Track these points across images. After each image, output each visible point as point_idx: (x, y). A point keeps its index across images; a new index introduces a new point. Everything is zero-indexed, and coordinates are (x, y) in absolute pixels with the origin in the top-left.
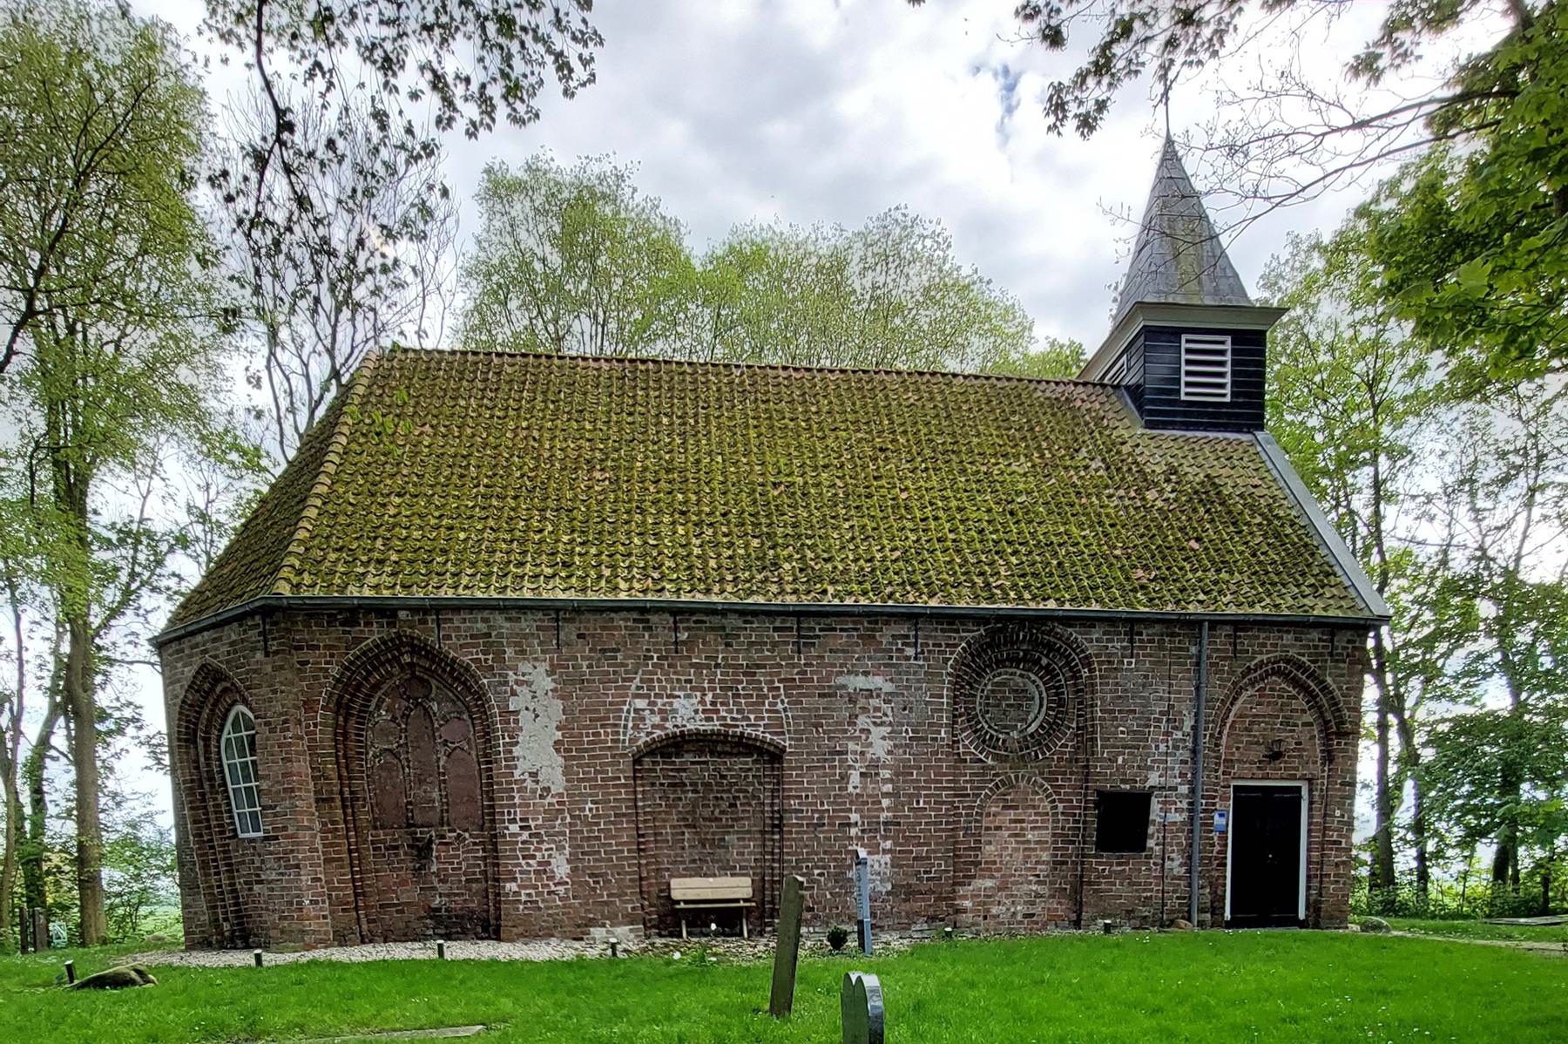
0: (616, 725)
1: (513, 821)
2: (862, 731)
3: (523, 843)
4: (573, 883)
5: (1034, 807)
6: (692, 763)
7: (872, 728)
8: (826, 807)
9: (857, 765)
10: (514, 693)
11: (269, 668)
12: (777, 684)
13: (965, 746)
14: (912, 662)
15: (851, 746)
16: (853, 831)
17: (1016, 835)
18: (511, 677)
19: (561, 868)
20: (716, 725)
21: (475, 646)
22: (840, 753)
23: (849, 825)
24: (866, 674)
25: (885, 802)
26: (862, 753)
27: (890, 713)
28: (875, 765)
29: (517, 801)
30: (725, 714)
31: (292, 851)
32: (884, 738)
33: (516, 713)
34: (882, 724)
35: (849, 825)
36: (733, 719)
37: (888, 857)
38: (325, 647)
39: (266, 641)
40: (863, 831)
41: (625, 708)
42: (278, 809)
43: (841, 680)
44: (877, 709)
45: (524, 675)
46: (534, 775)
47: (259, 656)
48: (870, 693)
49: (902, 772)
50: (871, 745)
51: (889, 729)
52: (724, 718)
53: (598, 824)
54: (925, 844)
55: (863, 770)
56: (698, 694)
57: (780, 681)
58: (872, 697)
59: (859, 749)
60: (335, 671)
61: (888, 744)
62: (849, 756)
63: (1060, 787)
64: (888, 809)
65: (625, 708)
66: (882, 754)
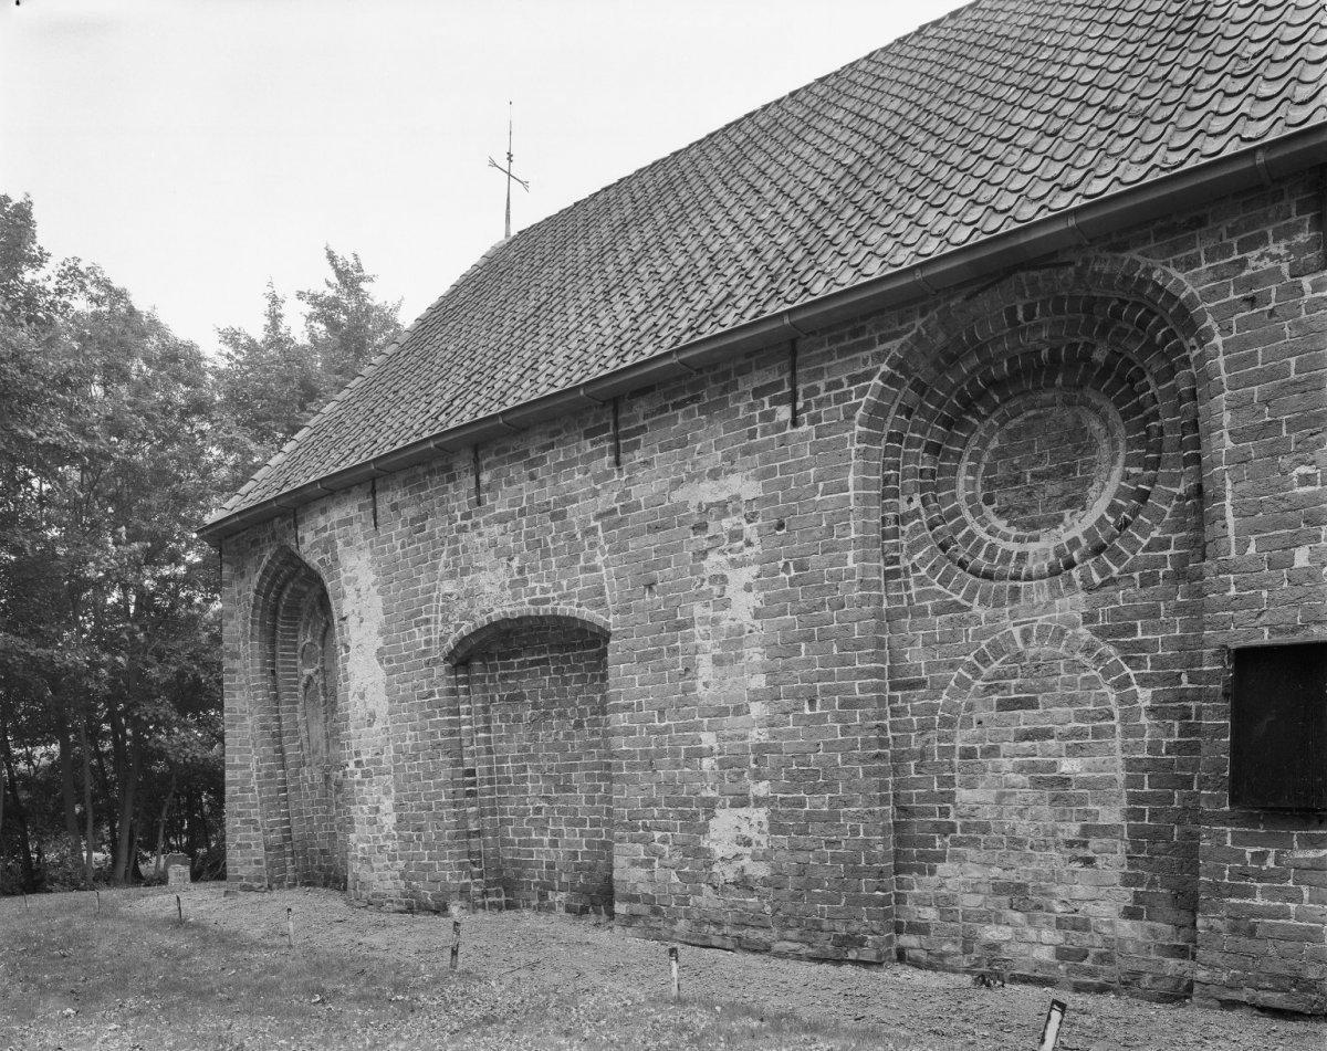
0: (427, 621)
2: (714, 579)
4: (400, 837)
5: (1072, 701)
7: (729, 574)
8: (667, 722)
9: (708, 644)
12: (593, 524)
13: (921, 581)
14: (788, 431)
15: (698, 610)
16: (707, 763)
17: (1034, 767)
19: (389, 821)
22: (681, 626)
23: (700, 754)
24: (715, 474)
25: (757, 709)
26: (715, 621)
27: (755, 539)
28: (736, 638)
30: (533, 585)
32: (748, 588)
34: (743, 564)
35: (700, 754)
36: (544, 590)
37: (761, 814)
40: (720, 762)
41: (435, 595)
43: (678, 496)
44: (736, 535)
48: (723, 508)
49: (784, 649)
50: (726, 605)
51: (755, 569)
52: (533, 591)
53: (416, 758)
54: (830, 786)
55: (718, 651)
56: (504, 560)
57: (599, 517)
58: (726, 514)
59: (710, 613)
61: (754, 600)
62: (698, 629)
63: (1141, 646)
64: (761, 723)
65: (435, 595)
66: (746, 618)
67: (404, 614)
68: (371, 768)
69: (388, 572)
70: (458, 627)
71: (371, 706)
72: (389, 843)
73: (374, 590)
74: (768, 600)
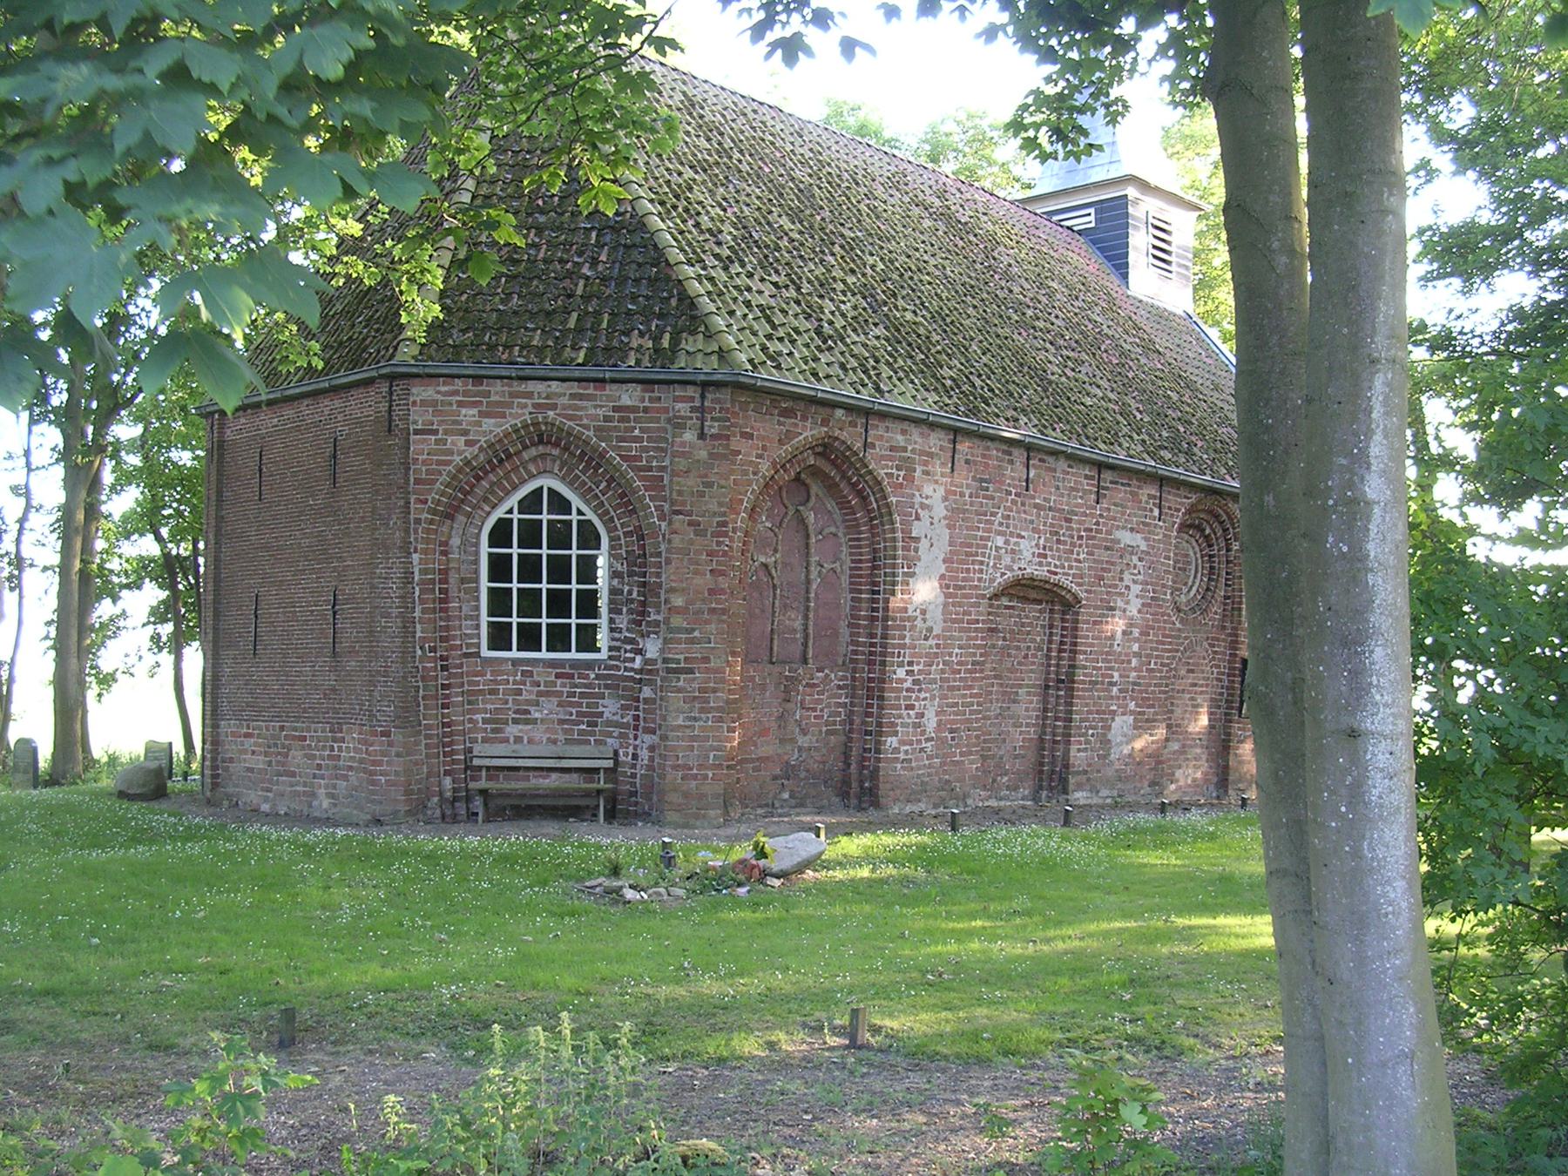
1: (901, 665)
3: (908, 690)
6: (1007, 607)
10: (918, 518)
11: (703, 454)
18: (917, 499)
19: (931, 722)
20: (1041, 573)
21: (891, 459)
23: (1112, 684)
29: (907, 641)
31: (715, 691)
33: (917, 540)
35: (1112, 684)
36: (1056, 566)
38: (762, 438)
39: (703, 420)
42: (696, 634)
45: (927, 497)
46: (924, 612)
47: (689, 436)
60: (765, 467)
67: (962, 555)
68: (921, 678)
69: (956, 515)
70: (1003, 574)
71: (929, 623)
72: (929, 744)
73: (944, 522)
74: (1143, 605)
